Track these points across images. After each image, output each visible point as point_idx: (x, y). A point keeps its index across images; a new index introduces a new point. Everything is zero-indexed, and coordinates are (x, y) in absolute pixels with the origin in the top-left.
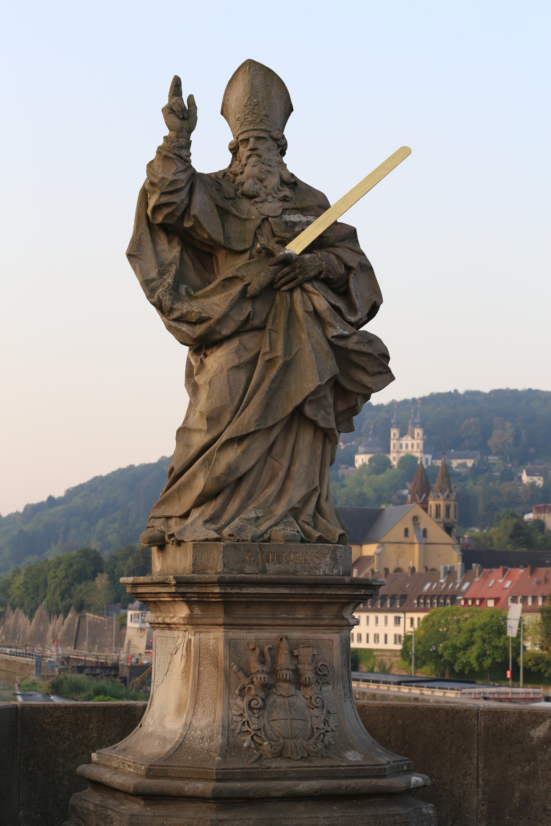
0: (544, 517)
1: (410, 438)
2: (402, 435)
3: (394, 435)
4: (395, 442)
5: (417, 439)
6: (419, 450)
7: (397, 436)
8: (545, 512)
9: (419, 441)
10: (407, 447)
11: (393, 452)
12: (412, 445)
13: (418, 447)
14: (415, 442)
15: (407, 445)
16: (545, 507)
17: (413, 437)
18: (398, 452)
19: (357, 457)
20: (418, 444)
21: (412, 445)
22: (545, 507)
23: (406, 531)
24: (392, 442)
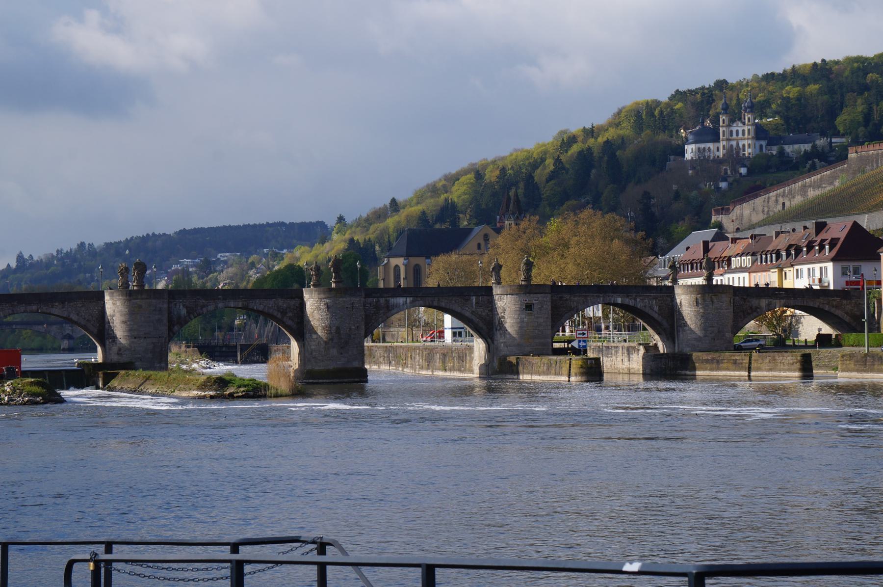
0: (722, 218)
1: (740, 124)
2: (732, 121)
3: (724, 121)
4: (724, 129)
5: (748, 125)
6: (750, 136)
7: (726, 122)
8: (722, 214)
9: (750, 127)
10: (737, 134)
11: (723, 140)
12: (743, 131)
13: (749, 134)
14: (746, 128)
15: (737, 131)
16: (722, 209)
17: (744, 124)
18: (728, 140)
19: (686, 147)
20: (749, 130)
21: (743, 131)
22: (722, 209)
23: (479, 245)
24: (721, 130)
